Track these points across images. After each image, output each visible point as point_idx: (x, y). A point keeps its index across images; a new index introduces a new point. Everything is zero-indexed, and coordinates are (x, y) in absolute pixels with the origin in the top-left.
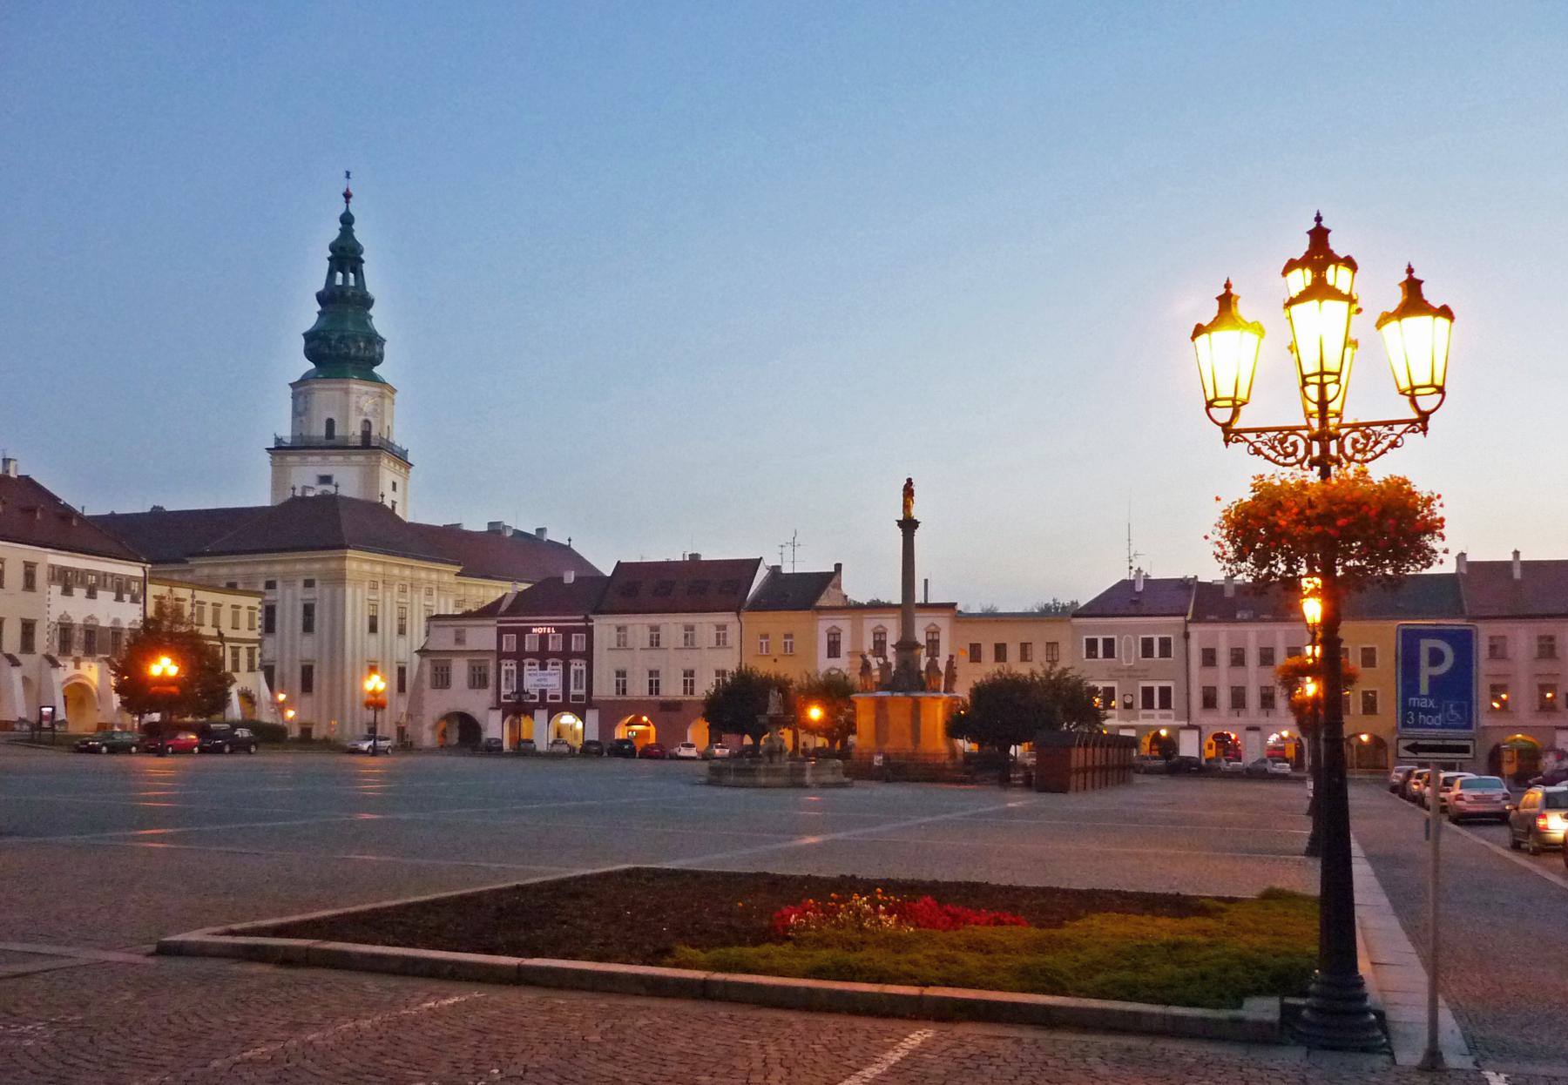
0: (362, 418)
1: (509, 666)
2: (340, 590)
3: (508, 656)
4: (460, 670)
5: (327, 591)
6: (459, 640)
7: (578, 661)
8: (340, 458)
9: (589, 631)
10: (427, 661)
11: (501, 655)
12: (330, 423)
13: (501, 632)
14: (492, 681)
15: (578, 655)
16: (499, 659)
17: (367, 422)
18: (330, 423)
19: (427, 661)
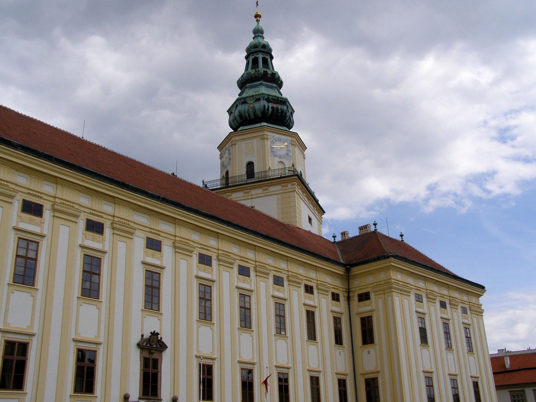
8: (259, 191)
12: (250, 165)
18: (250, 165)
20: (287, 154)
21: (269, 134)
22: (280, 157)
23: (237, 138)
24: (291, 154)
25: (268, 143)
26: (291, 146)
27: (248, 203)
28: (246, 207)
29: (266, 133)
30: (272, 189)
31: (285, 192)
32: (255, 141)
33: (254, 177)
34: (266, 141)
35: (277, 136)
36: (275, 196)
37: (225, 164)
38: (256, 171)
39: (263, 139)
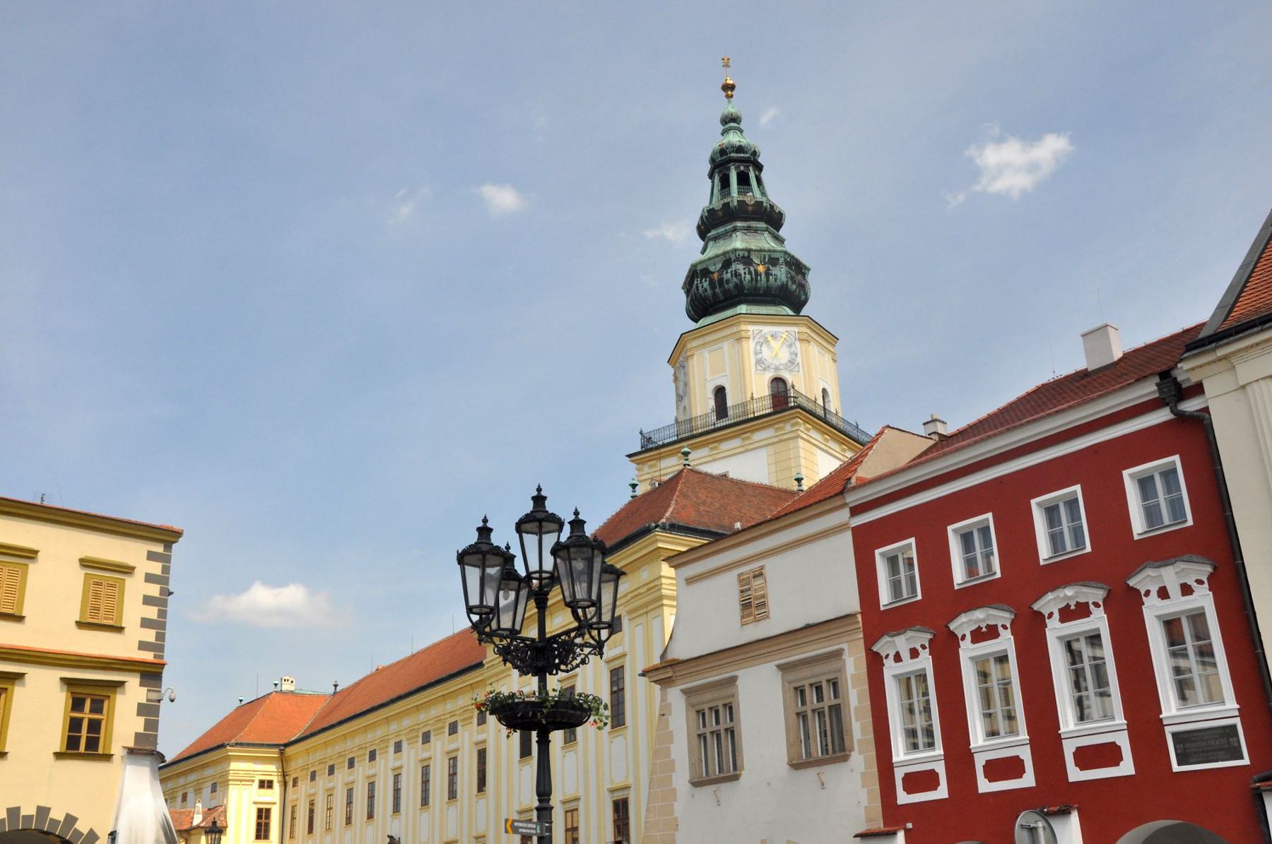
0: (769, 375)
1: (907, 655)
2: (656, 622)
3: (898, 620)
4: (762, 699)
5: (639, 629)
6: (752, 606)
7: (1170, 576)
8: (736, 443)
9: (1195, 438)
10: (675, 695)
11: (877, 622)
12: (720, 392)
13: (866, 541)
14: (859, 728)
15: (1162, 549)
16: (870, 639)
17: (778, 381)
18: (720, 392)
19: (675, 695)
20: (792, 362)
21: (751, 328)
22: (777, 369)
23: (694, 344)
24: (799, 359)
25: (750, 346)
26: (797, 343)
27: (714, 469)
28: (712, 476)
29: (743, 327)
30: (758, 436)
31: (781, 441)
32: (726, 345)
33: (726, 416)
34: (744, 342)
35: (767, 329)
36: (764, 451)
37: (681, 392)
38: (730, 403)
39: (739, 339)
